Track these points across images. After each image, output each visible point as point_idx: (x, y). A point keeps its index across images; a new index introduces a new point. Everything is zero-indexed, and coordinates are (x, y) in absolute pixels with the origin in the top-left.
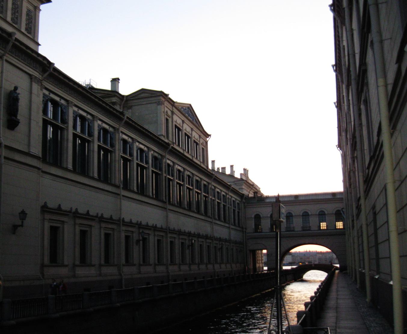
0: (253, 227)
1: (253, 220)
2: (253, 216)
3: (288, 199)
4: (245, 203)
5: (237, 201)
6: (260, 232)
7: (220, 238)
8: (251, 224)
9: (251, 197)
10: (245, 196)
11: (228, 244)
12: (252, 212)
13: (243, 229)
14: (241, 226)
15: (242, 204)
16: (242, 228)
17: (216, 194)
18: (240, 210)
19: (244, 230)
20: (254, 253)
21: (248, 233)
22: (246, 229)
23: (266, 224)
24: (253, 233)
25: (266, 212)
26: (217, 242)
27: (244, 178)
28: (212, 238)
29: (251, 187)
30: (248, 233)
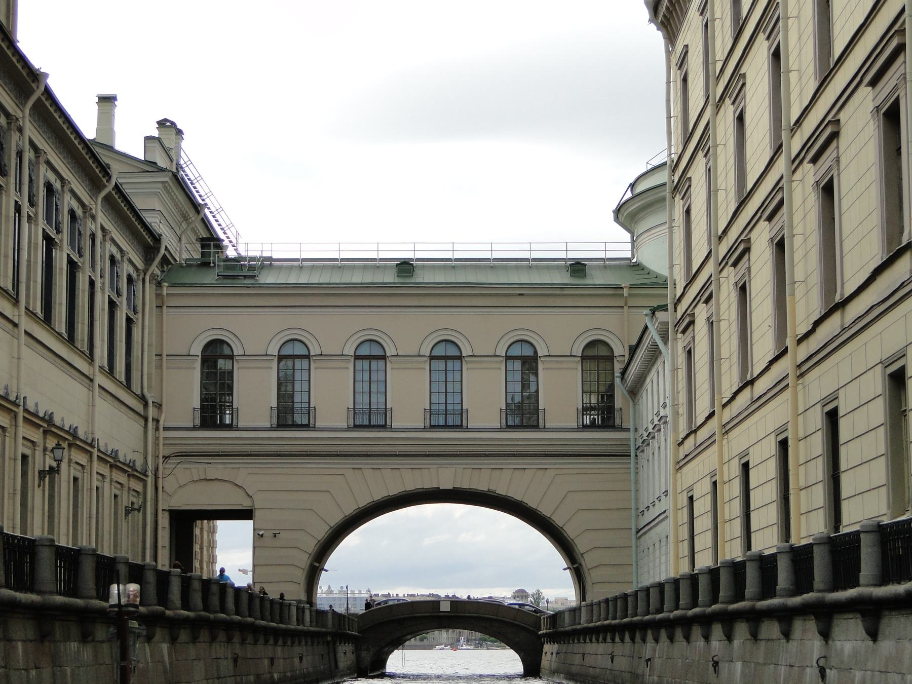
0: (197, 403)
1: (198, 364)
2: (197, 350)
3: (368, 278)
4: (159, 284)
5: (126, 269)
6: (230, 427)
7: (49, 420)
8: (184, 391)
9: (189, 265)
10: (163, 251)
11: (82, 459)
12: (188, 327)
13: (145, 410)
14: (136, 387)
15: (147, 284)
16: (146, 405)
17: (42, 193)
18: (135, 312)
19: (152, 412)
20: (186, 525)
21: (165, 429)
22: (159, 406)
23: (254, 395)
24: (194, 428)
25: (254, 333)
26: (36, 435)
27: (162, 162)
28: (14, 403)
29: (191, 213)
30: (165, 429)
